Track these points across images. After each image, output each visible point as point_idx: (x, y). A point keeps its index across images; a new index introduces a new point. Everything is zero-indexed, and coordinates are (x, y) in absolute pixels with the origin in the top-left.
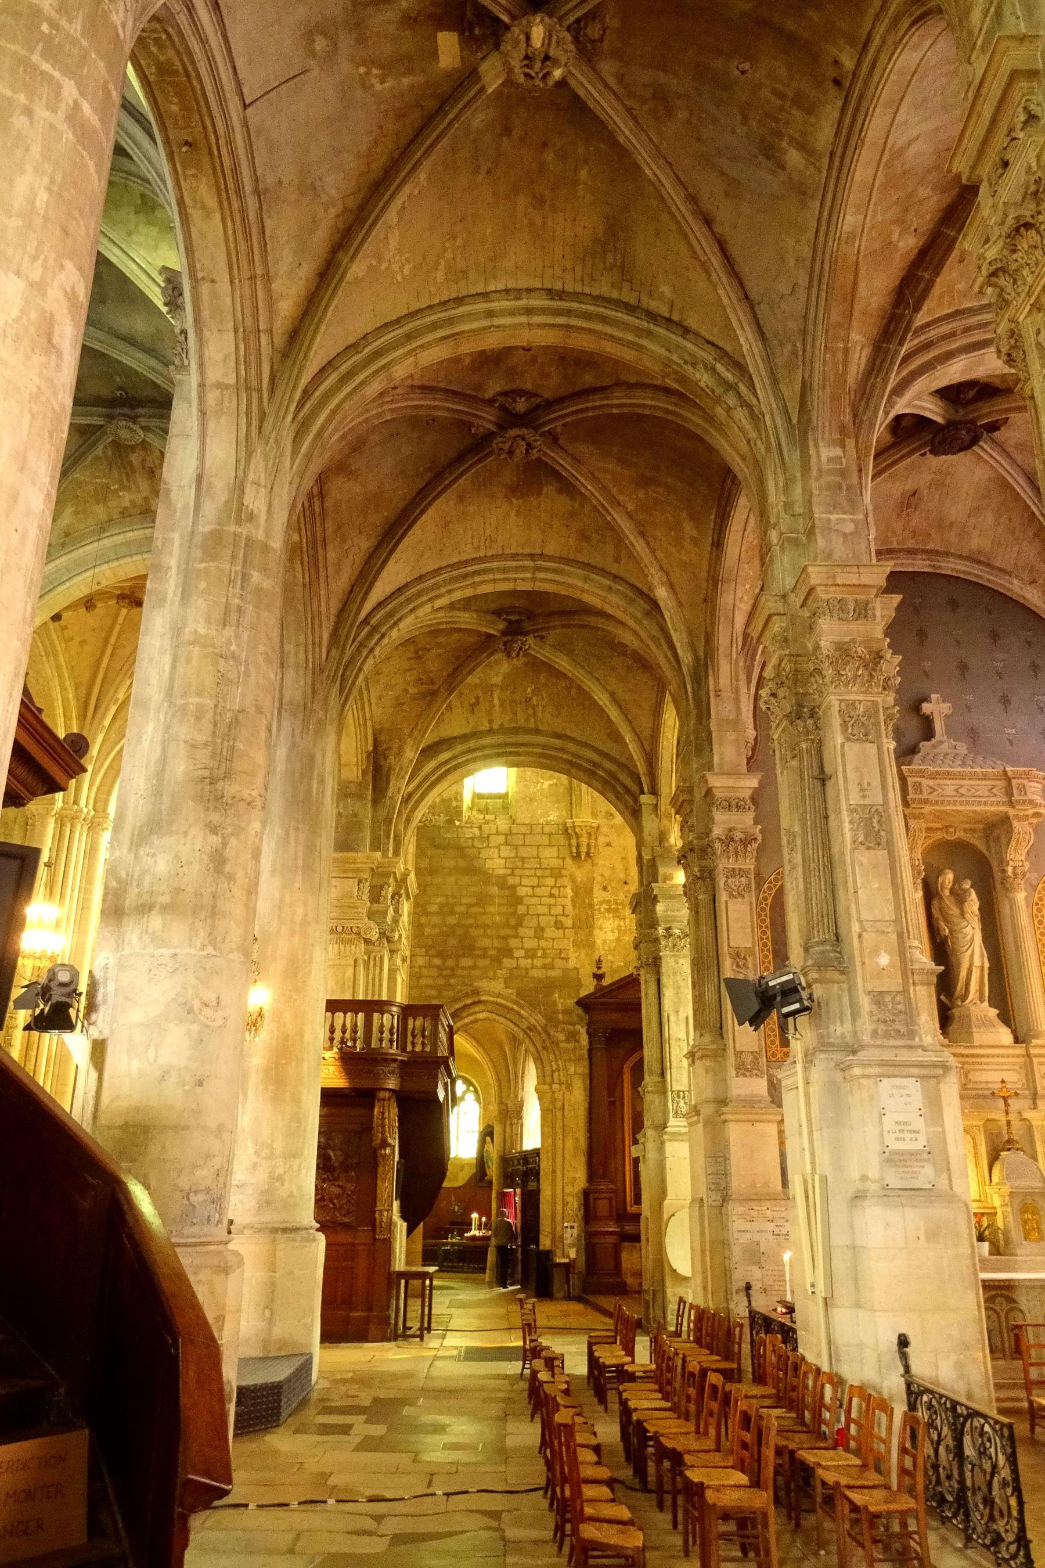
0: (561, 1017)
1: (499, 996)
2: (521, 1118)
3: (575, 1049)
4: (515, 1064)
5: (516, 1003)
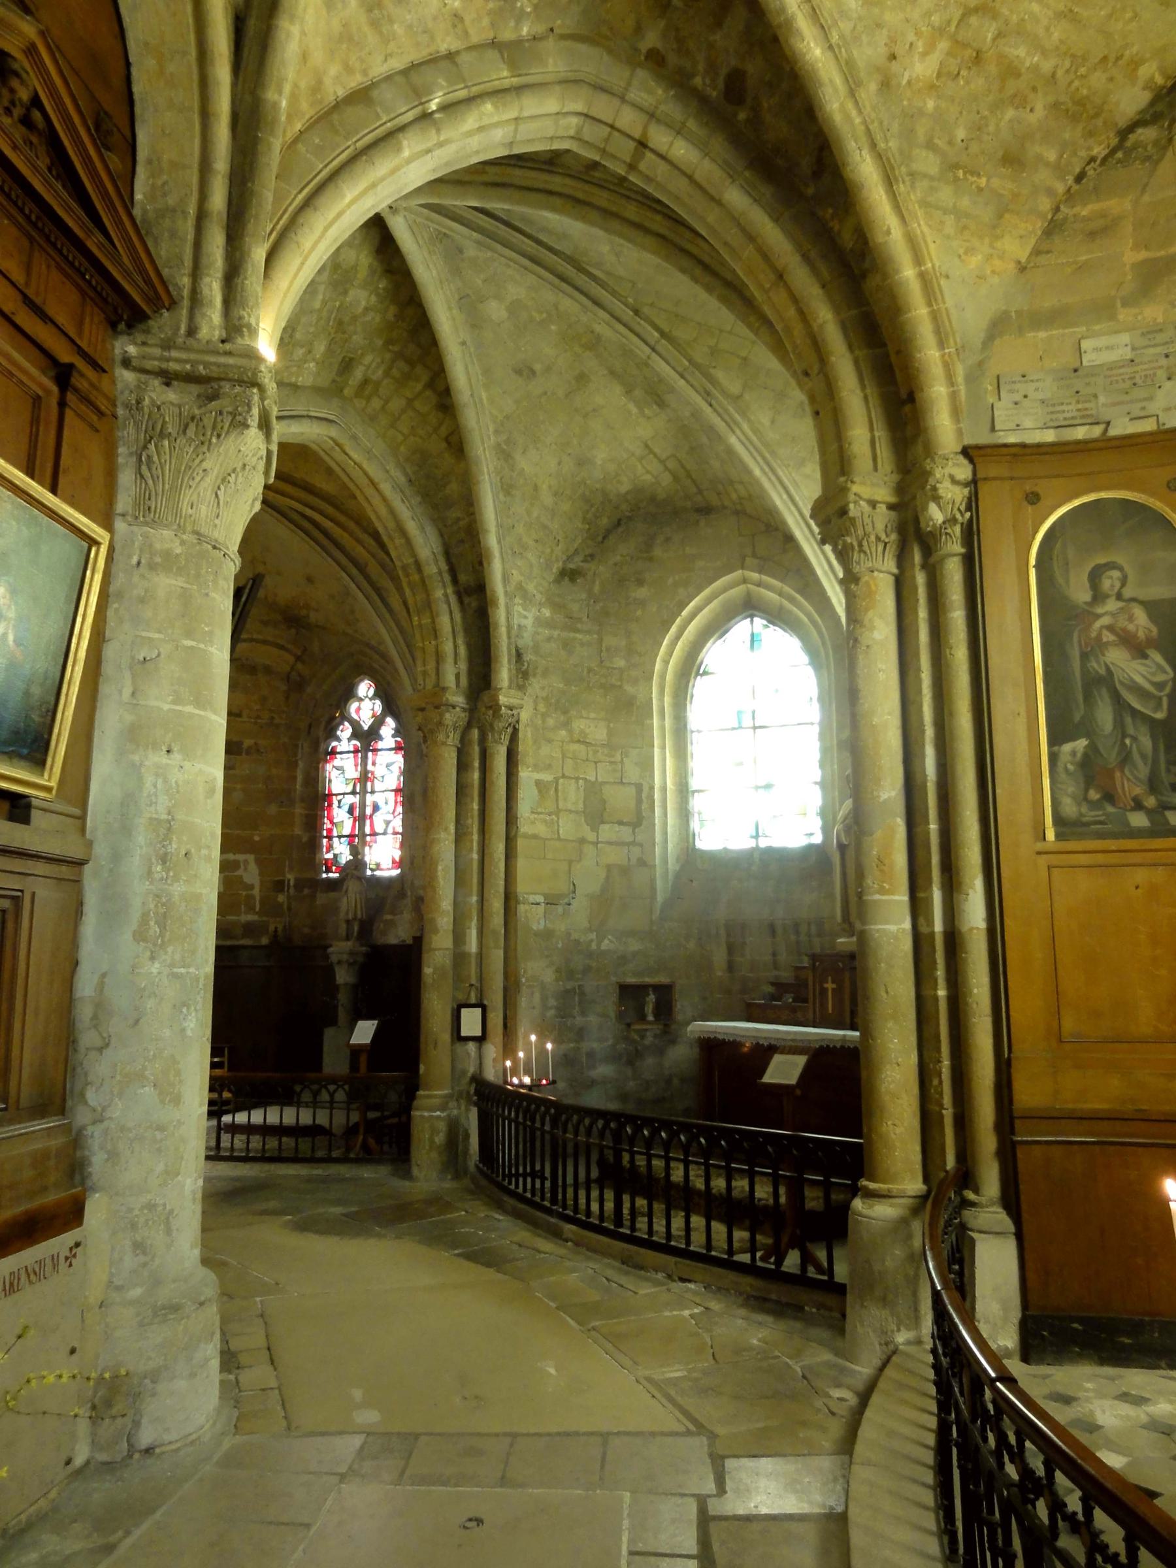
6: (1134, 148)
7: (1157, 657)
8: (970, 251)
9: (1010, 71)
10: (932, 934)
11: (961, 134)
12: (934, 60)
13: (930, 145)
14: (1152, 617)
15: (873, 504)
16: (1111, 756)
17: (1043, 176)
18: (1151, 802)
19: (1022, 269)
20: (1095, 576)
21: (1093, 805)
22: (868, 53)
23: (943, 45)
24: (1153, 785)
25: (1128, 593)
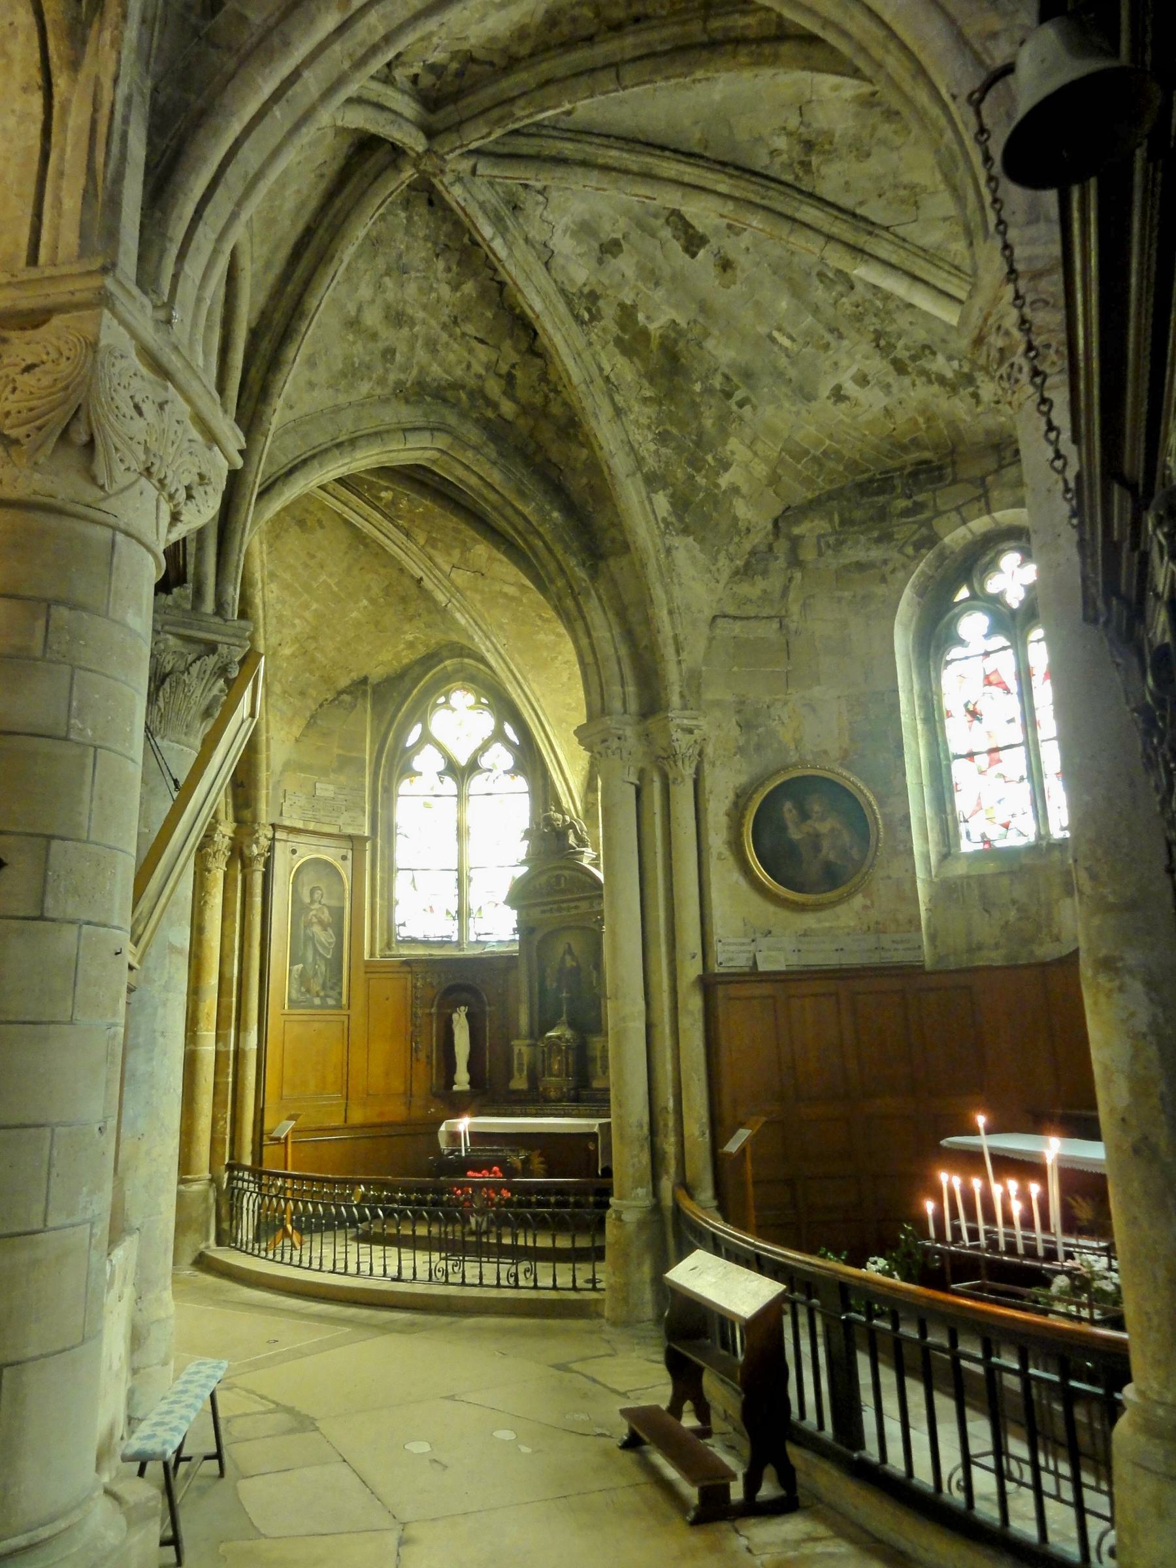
6: (341, 702)
7: (330, 931)
8: (282, 729)
9: (313, 660)
10: (228, 1052)
11: (290, 679)
12: (293, 649)
13: (280, 682)
14: (330, 914)
15: (224, 836)
16: (311, 973)
17: (310, 702)
18: (322, 994)
19: (297, 740)
20: (312, 892)
21: (303, 994)
22: (273, 641)
23: (297, 645)
24: (324, 987)
25: (323, 901)
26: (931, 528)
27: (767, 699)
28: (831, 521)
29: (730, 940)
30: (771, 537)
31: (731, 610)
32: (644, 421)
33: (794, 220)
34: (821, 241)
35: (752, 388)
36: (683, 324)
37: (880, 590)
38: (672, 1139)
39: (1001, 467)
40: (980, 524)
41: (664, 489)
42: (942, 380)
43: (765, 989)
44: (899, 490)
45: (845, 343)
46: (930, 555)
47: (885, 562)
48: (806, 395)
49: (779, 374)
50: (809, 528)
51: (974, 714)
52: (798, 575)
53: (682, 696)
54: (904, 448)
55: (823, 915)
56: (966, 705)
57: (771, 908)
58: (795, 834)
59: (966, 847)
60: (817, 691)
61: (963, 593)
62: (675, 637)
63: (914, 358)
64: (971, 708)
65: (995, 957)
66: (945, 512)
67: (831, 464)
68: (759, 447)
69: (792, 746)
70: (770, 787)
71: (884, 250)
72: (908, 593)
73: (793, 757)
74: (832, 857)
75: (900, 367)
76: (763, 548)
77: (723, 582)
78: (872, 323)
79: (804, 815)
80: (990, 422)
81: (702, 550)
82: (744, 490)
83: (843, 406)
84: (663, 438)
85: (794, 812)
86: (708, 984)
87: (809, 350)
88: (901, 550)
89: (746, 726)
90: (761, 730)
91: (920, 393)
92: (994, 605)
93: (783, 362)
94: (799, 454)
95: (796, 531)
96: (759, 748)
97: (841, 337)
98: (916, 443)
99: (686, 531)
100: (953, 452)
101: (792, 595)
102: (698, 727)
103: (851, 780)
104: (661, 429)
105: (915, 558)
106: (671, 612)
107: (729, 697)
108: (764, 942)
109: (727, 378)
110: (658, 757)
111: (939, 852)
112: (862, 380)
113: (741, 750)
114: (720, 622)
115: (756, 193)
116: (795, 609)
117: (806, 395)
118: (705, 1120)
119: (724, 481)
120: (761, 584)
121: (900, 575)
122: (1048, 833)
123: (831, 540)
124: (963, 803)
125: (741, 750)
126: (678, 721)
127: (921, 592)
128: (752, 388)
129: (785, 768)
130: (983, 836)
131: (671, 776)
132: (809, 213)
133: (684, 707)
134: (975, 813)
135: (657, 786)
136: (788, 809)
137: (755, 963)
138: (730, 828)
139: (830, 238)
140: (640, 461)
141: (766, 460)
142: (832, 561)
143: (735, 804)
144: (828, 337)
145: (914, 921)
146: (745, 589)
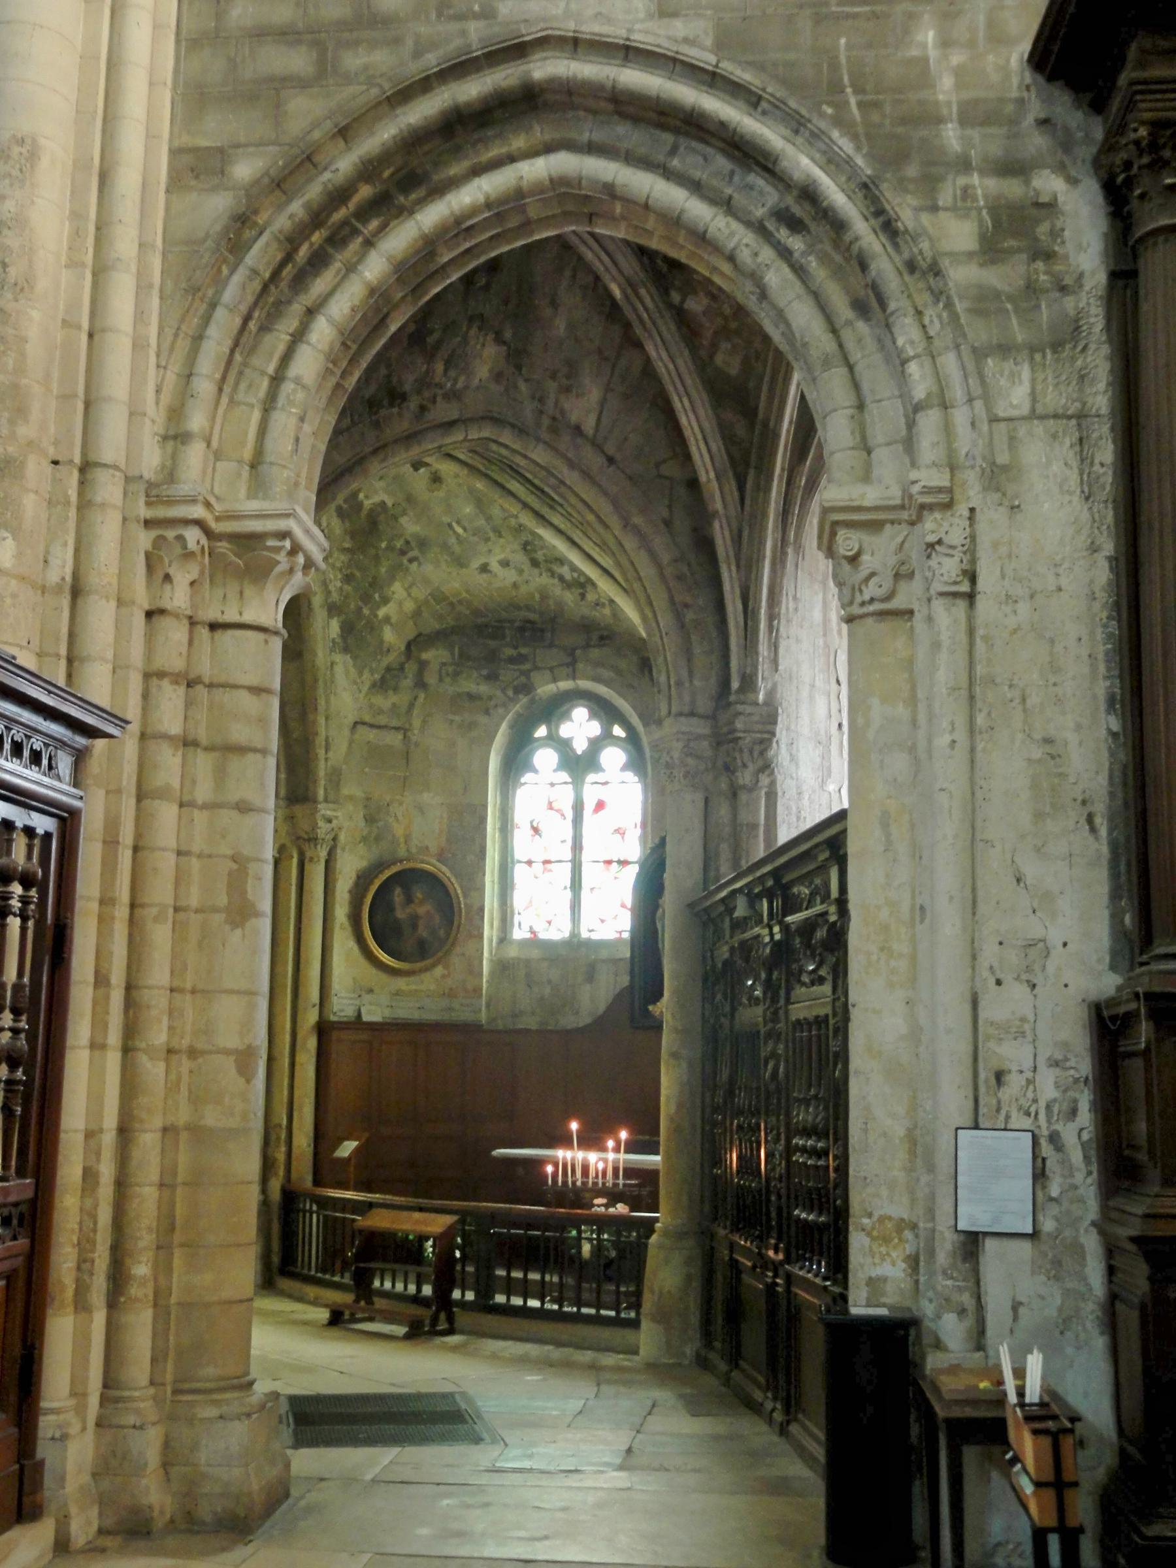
0: (951, 136)
1: (629, 53)
2: (767, 767)
3: (1031, 289)
4: (748, 566)
5: (712, 79)
26: (528, 678)
27: (388, 798)
28: (452, 654)
29: (343, 995)
30: (403, 659)
31: (367, 718)
32: (338, 565)
33: (503, 487)
34: (520, 506)
35: (423, 553)
36: (389, 503)
37: (483, 719)
38: (283, 1149)
39: (588, 646)
40: (565, 685)
41: (339, 615)
42: (561, 578)
43: (363, 1036)
44: (508, 639)
45: (502, 540)
46: (524, 700)
47: (490, 698)
48: (460, 562)
49: (445, 547)
50: (434, 656)
51: (536, 830)
52: (422, 696)
53: (326, 789)
54: (518, 608)
55: (412, 979)
56: (531, 822)
57: (374, 971)
58: (401, 914)
59: (518, 934)
60: (426, 797)
61: (541, 731)
62: (327, 738)
63: (546, 561)
64: (535, 825)
65: (530, 1023)
66: (544, 668)
67: (459, 608)
68: (415, 592)
69: (402, 840)
70: (387, 874)
71: (556, 520)
72: (504, 727)
73: (402, 852)
74: (425, 934)
75: (535, 563)
76: (396, 665)
77: (364, 692)
78: (525, 537)
79: (409, 900)
80: (586, 611)
81: (354, 665)
82: (393, 620)
83: (484, 576)
84: (348, 579)
85: (402, 897)
86: (323, 1029)
87: (476, 539)
88: (503, 690)
89: (370, 819)
90: (381, 824)
91: (545, 580)
92: (563, 747)
93: (452, 540)
94: (438, 596)
95: (425, 656)
96: (378, 839)
97: (500, 536)
98: (528, 608)
99: (346, 650)
100: (553, 620)
101: (415, 712)
102: (337, 817)
103: (444, 872)
104: (349, 571)
105: (511, 700)
106: (327, 718)
107: (359, 793)
108: (367, 998)
109: (407, 542)
110: (298, 838)
111: (498, 936)
112: (505, 564)
113: (364, 839)
114: (361, 730)
115: (484, 465)
116: (417, 723)
117: (460, 562)
118: (312, 1134)
119: (381, 613)
120: (393, 698)
121: (501, 711)
122: (579, 933)
123: (450, 669)
124: (519, 899)
125: (364, 839)
126: (323, 812)
127: (511, 727)
128: (423, 553)
129: (401, 861)
130: (531, 928)
131: (308, 854)
132: (514, 486)
133: (326, 800)
134: (527, 908)
135: (295, 861)
136: (398, 895)
137: (359, 1015)
138: (351, 903)
139: (525, 505)
140: (328, 593)
141: (416, 600)
142: (449, 688)
143: (357, 884)
144: (491, 534)
145: (477, 990)
146: (380, 701)
